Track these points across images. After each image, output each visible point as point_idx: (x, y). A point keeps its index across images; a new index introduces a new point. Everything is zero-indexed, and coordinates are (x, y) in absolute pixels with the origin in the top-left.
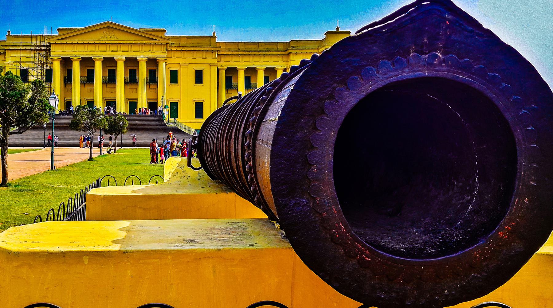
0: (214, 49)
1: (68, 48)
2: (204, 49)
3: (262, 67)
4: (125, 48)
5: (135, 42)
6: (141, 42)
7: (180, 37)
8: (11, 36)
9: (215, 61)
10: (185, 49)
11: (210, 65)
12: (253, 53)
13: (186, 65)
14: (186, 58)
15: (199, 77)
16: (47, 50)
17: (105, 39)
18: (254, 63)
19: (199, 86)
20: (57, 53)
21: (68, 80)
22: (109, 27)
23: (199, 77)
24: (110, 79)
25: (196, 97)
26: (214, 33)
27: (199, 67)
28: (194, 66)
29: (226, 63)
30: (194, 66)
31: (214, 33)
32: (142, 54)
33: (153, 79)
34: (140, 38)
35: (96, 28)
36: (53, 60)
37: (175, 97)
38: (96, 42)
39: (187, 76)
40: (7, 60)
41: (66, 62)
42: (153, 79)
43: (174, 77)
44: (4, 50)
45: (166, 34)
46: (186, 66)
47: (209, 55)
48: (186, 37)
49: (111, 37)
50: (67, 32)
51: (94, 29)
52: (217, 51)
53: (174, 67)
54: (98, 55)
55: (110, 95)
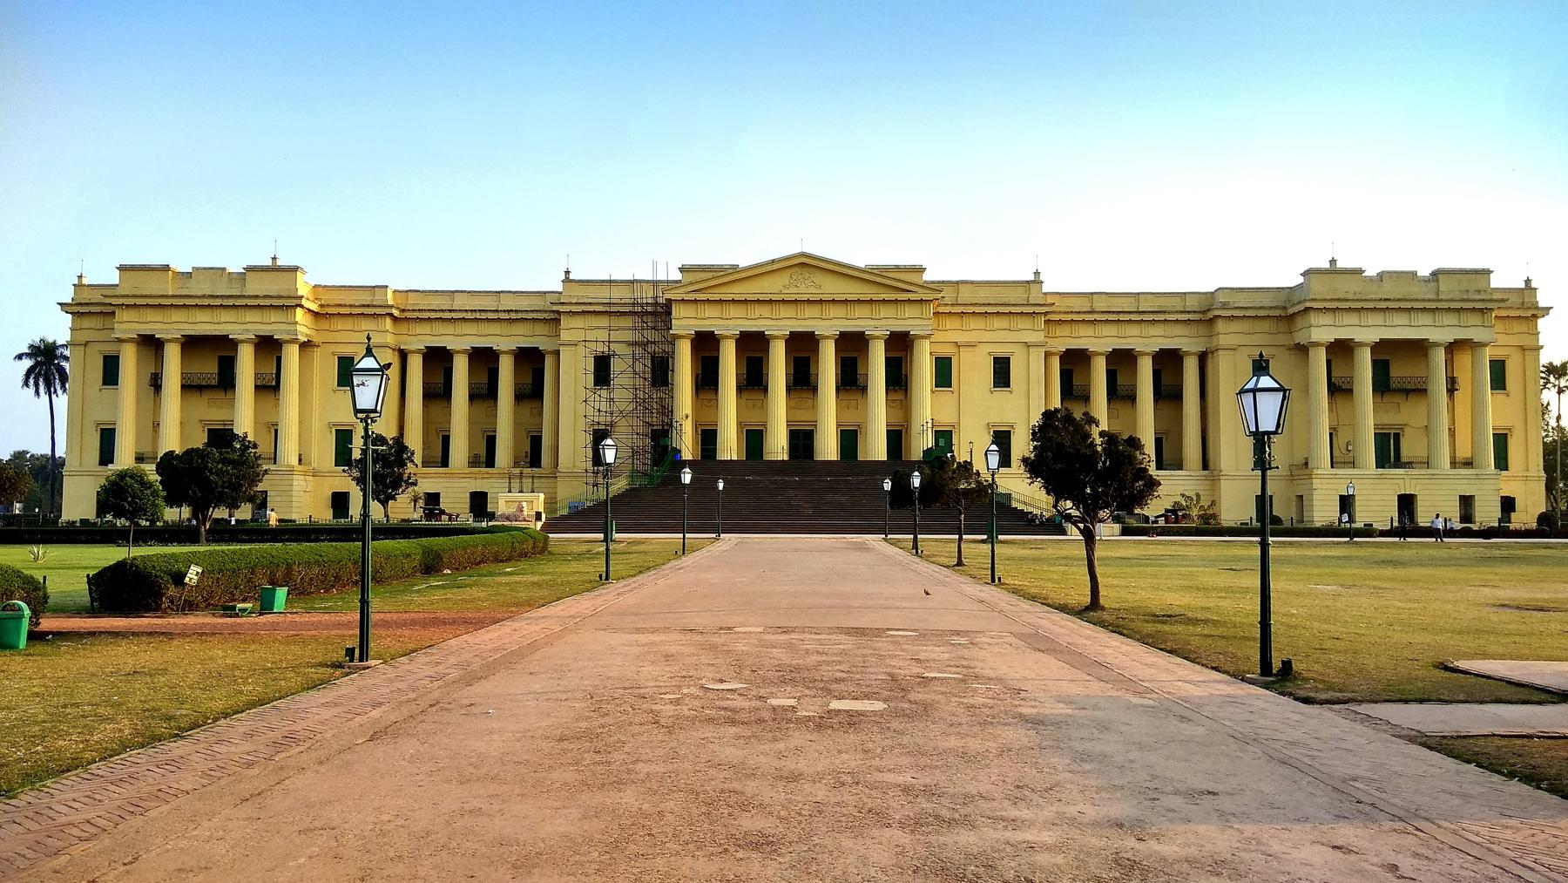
0: (1037, 309)
1: (710, 311)
2: (1014, 309)
3: (1148, 350)
7: (957, 282)
11: (1028, 345)
12: (1127, 317)
14: (974, 330)
15: (1002, 373)
16: (661, 313)
19: (1002, 393)
20: (685, 322)
21: (707, 380)
22: (803, 265)
23: (1002, 373)
24: (802, 380)
25: (997, 419)
26: (1037, 273)
27: (1002, 351)
28: (990, 348)
29: (1066, 340)
30: (990, 348)
31: (1037, 273)
33: (898, 379)
34: (874, 289)
35: (775, 267)
36: (676, 337)
39: (974, 372)
40: (565, 336)
41: (706, 344)
42: (898, 379)
43: (944, 373)
44: (558, 312)
45: (927, 277)
47: (1023, 323)
48: (972, 282)
49: (807, 287)
50: (710, 275)
51: (769, 268)
52: (1046, 313)
53: (945, 351)
54: (778, 325)
55: (803, 416)
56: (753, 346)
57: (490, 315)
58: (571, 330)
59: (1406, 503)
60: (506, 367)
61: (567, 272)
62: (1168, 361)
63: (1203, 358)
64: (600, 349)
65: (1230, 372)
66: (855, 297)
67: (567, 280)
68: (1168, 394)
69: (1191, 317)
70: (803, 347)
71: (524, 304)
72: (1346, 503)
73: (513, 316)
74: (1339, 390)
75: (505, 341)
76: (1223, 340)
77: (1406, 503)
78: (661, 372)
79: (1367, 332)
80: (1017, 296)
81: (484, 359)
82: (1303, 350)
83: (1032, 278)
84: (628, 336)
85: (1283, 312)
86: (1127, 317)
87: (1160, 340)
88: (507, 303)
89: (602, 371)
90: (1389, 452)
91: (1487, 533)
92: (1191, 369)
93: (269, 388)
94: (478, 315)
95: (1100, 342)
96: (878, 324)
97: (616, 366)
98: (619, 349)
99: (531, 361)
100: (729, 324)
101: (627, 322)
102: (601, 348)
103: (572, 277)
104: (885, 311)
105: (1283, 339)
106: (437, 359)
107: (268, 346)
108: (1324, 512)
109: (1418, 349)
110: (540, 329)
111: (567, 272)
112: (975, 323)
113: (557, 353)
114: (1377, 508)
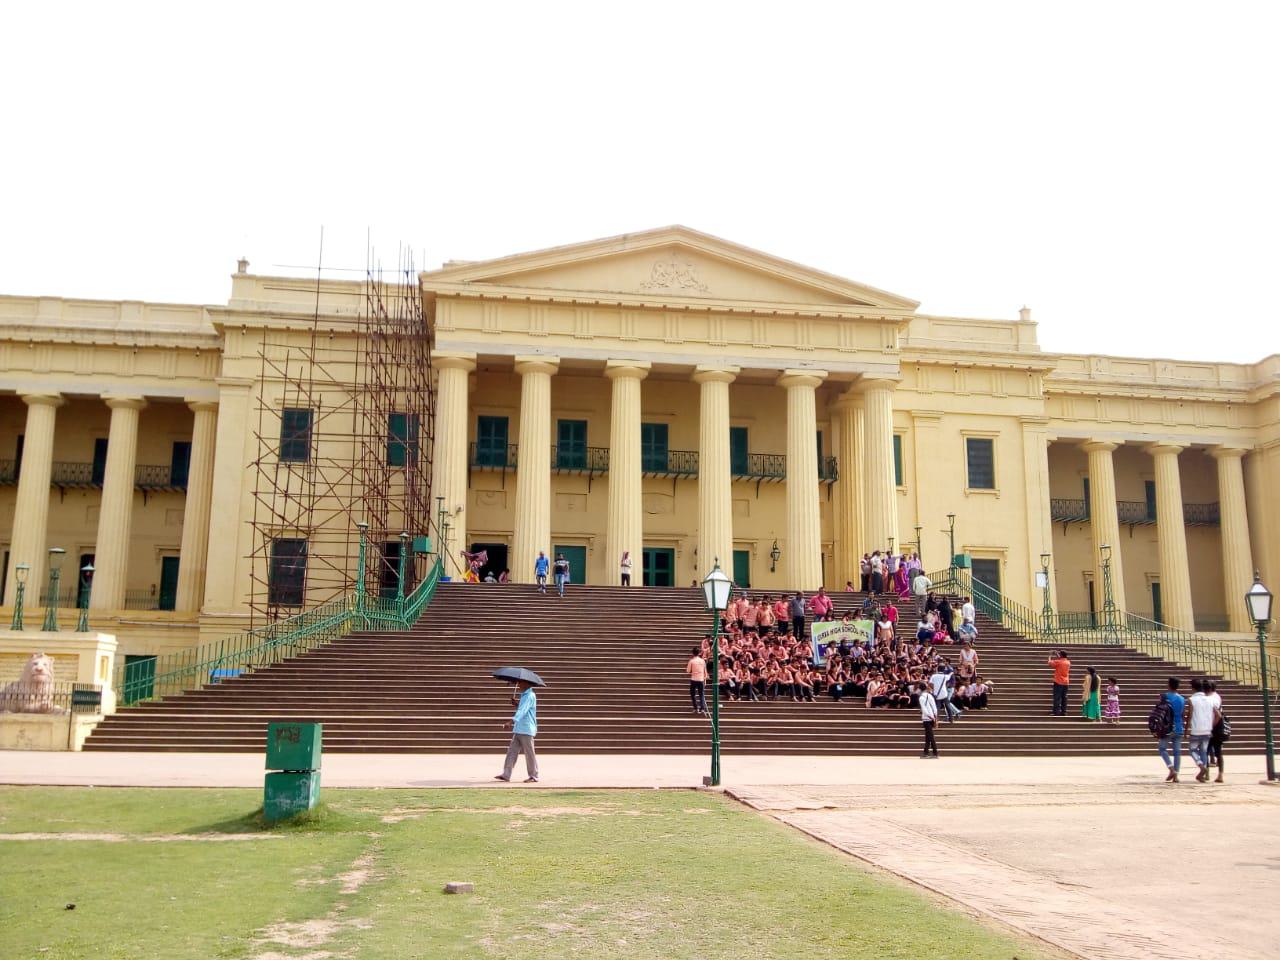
1: (504, 319)
4: (740, 332)
5: (782, 309)
6: (804, 310)
8: (252, 278)
9: (1037, 408)
10: (931, 359)
11: (1021, 421)
13: (934, 416)
17: (663, 291)
18: (1146, 429)
19: (981, 499)
20: (459, 340)
22: (676, 249)
27: (980, 428)
35: (629, 247)
38: (627, 301)
40: (230, 369)
46: (934, 423)
47: (1015, 385)
51: (618, 249)
54: (630, 352)
56: (582, 386)
57: (101, 340)
58: (240, 360)
60: (122, 434)
61: (243, 263)
62: (1199, 463)
64: (292, 396)
66: (768, 309)
69: (1234, 398)
71: (164, 323)
73: (142, 341)
75: (123, 385)
78: (404, 439)
80: (999, 342)
83: (1017, 317)
84: (345, 374)
86: (1143, 393)
87: (1192, 431)
88: (131, 321)
89: (296, 435)
92: (1230, 475)
94: (78, 338)
95: (1105, 429)
96: (805, 360)
98: (331, 398)
99: (170, 425)
101: (346, 352)
102: (296, 399)
103: (250, 271)
110: (189, 366)
111: (243, 263)
112: (941, 381)
113: (214, 409)
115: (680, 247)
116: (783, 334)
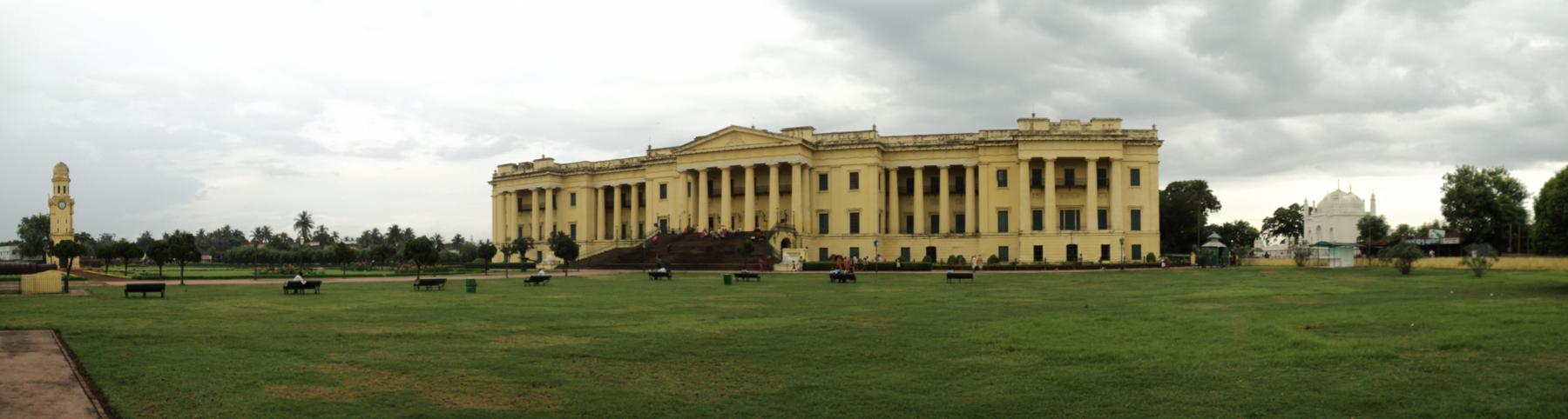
4: (753, 154)
11: (870, 165)
15: (854, 181)
19: (854, 193)
23: (854, 181)
27: (854, 169)
32: (772, 159)
37: (824, 206)
39: (839, 181)
53: (824, 170)
54: (723, 163)
59: (1072, 250)
60: (634, 193)
62: (957, 173)
63: (976, 169)
65: (987, 178)
67: (650, 150)
68: (958, 190)
70: (737, 172)
72: (1038, 251)
74: (1037, 183)
76: (983, 159)
77: (1072, 250)
79: (1050, 153)
81: (625, 189)
82: (1019, 162)
85: (1012, 142)
90: (1070, 220)
91: (1122, 266)
93: (542, 209)
95: (917, 162)
97: (669, 190)
100: (702, 165)
104: (779, 152)
105: (1014, 158)
106: (609, 191)
107: (541, 191)
108: (1027, 257)
109: (1082, 162)
114: (1055, 253)
115: (733, 132)
116: (765, 153)
